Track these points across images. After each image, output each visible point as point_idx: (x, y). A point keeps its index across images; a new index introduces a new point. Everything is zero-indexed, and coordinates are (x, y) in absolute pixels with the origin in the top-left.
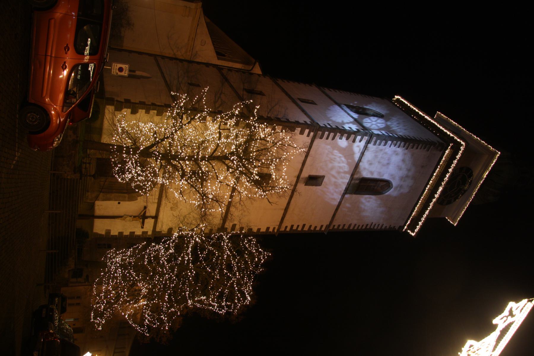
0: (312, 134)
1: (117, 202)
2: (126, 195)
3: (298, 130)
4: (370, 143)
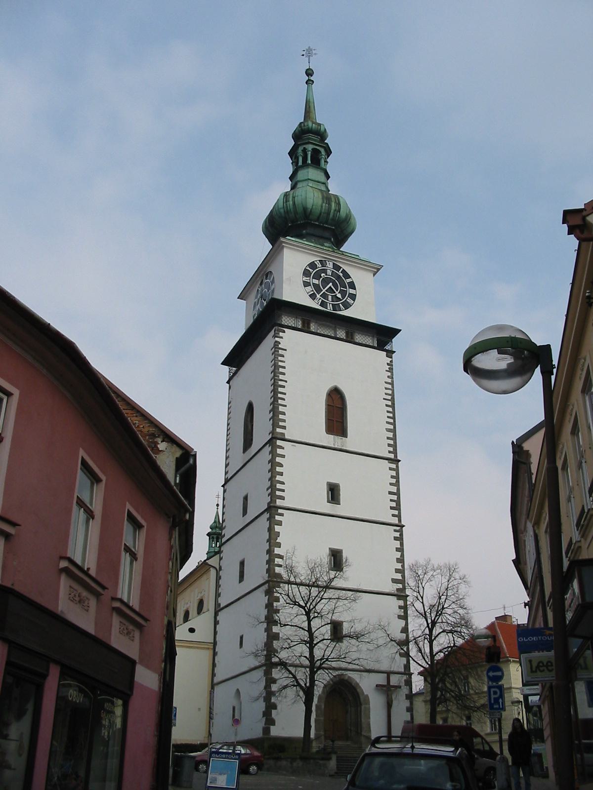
0: (280, 511)
2: (363, 707)
3: (277, 528)
4: (283, 434)
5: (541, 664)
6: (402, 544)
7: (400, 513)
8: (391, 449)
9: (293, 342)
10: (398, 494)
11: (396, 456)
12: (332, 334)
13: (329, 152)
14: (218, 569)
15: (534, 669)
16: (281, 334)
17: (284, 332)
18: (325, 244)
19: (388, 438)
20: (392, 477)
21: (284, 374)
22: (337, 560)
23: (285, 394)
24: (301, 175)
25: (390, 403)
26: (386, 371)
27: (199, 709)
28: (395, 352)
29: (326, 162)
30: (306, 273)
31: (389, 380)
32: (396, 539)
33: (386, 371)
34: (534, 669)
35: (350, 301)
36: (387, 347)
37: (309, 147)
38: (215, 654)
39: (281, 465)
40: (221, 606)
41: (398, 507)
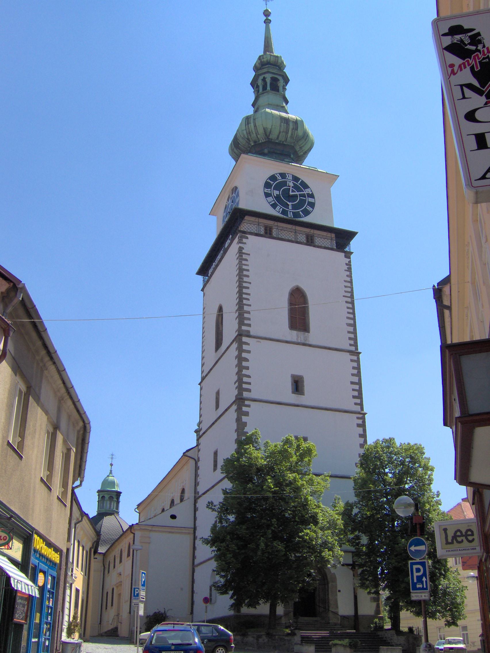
0: (247, 402)
1: (338, 593)
2: (330, 585)
3: (244, 419)
4: (248, 332)
5: (458, 534)
6: (365, 431)
7: (362, 401)
8: (352, 342)
9: (258, 248)
10: (359, 383)
11: (357, 349)
12: (292, 236)
13: (287, 80)
14: (196, 459)
15: (450, 540)
16: (244, 240)
17: (247, 238)
18: (285, 160)
19: (349, 332)
20: (354, 368)
21: (248, 276)
23: (249, 294)
24: (261, 101)
25: (349, 300)
26: (345, 270)
27: (182, 589)
28: (353, 253)
29: (284, 89)
30: (267, 185)
31: (348, 279)
32: (358, 425)
33: (345, 270)
34: (450, 540)
36: (347, 249)
37: (270, 77)
38: (195, 538)
39: (247, 360)
40: (200, 494)
41: (360, 396)
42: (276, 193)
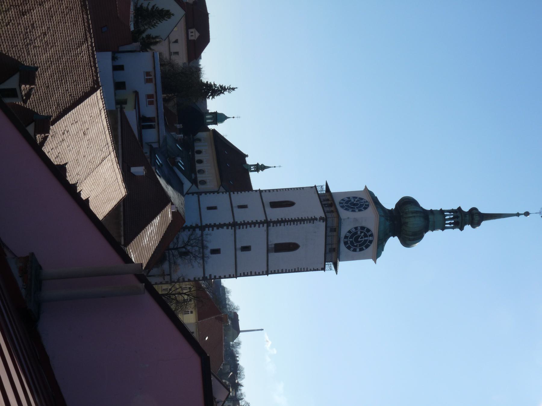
0: (233, 228)
3: (225, 227)
22: (216, 251)
30: (363, 228)
35: (352, 249)
42: (359, 233)
